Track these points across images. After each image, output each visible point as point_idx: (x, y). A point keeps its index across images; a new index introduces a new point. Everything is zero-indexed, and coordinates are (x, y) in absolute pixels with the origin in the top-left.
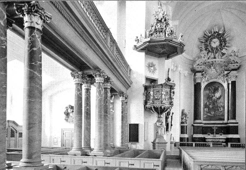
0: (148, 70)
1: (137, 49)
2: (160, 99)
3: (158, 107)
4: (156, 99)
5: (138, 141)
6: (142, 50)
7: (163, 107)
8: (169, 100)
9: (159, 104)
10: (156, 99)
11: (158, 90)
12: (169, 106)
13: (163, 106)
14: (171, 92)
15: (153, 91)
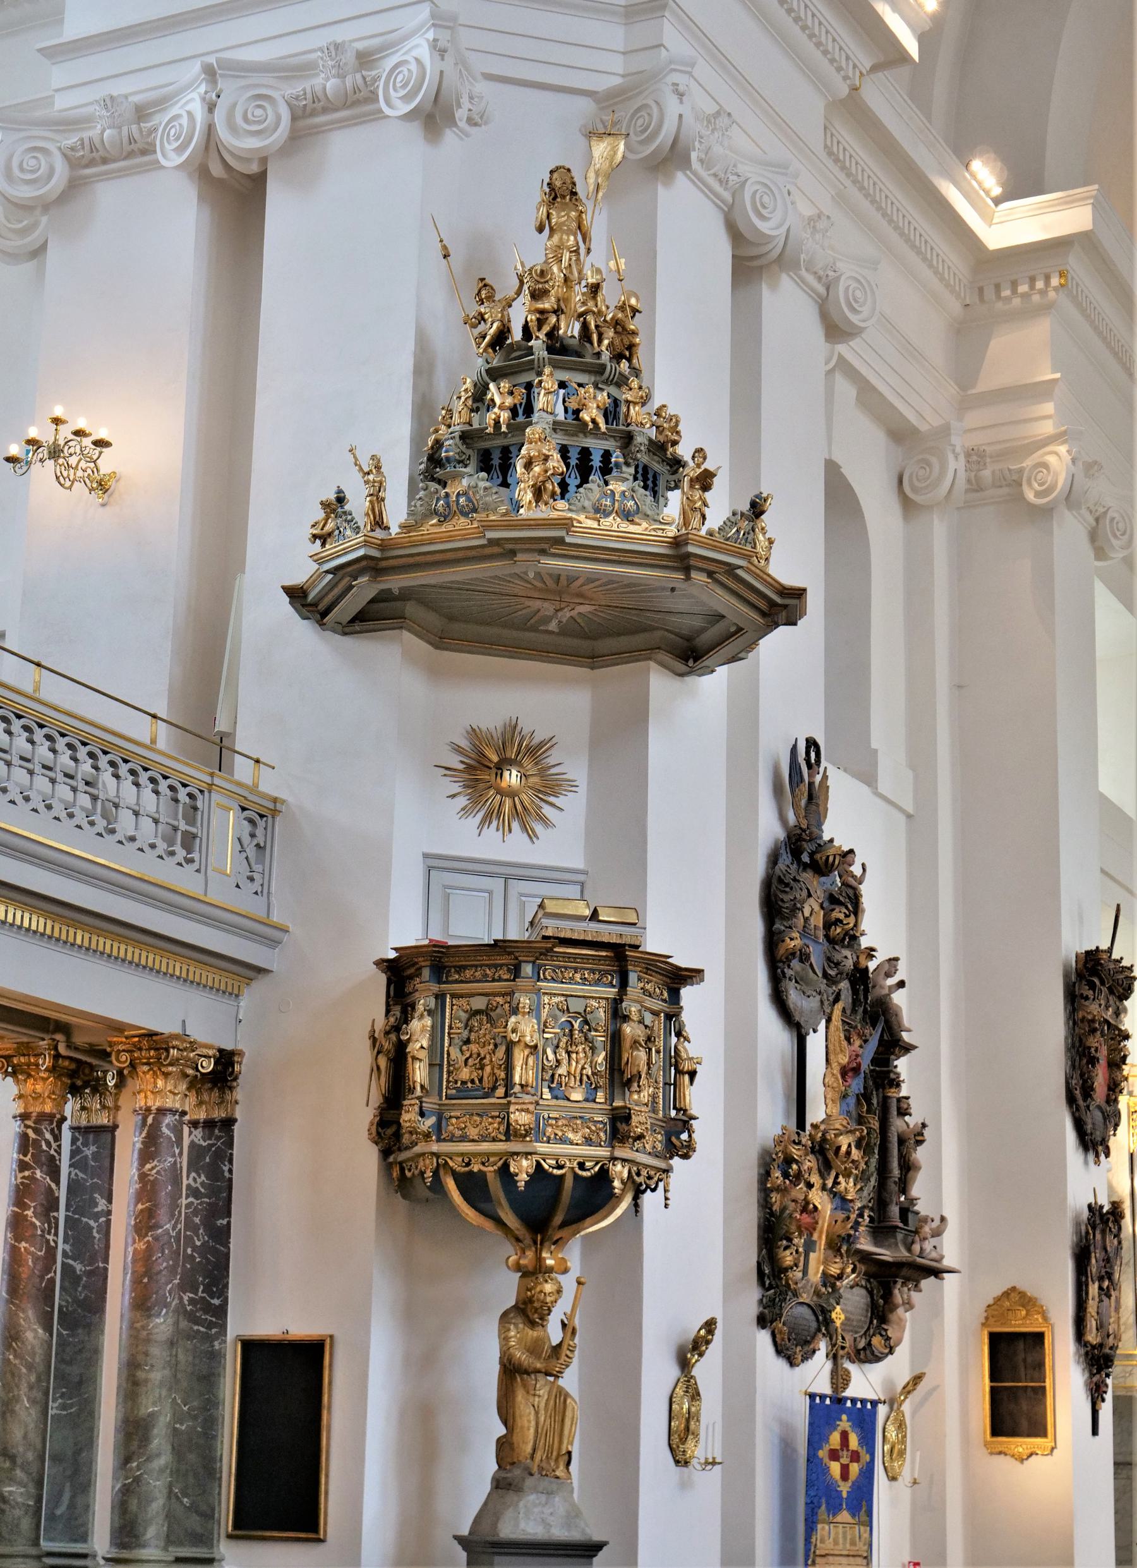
0: (462, 801)
1: (324, 614)
2: (500, 1091)
3: (476, 1168)
4: (463, 1091)
5: (314, 1528)
6: (357, 627)
7: (522, 1169)
8: (600, 1097)
9: (483, 1139)
10: (463, 1091)
11: (479, 1003)
12: (603, 1152)
13: (527, 1154)
14: (626, 1018)
15: (434, 1012)
